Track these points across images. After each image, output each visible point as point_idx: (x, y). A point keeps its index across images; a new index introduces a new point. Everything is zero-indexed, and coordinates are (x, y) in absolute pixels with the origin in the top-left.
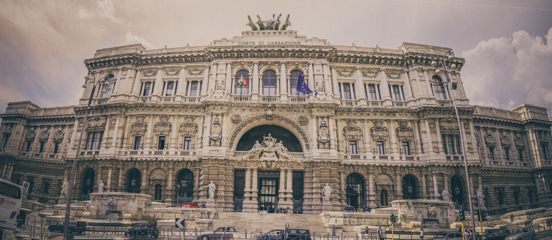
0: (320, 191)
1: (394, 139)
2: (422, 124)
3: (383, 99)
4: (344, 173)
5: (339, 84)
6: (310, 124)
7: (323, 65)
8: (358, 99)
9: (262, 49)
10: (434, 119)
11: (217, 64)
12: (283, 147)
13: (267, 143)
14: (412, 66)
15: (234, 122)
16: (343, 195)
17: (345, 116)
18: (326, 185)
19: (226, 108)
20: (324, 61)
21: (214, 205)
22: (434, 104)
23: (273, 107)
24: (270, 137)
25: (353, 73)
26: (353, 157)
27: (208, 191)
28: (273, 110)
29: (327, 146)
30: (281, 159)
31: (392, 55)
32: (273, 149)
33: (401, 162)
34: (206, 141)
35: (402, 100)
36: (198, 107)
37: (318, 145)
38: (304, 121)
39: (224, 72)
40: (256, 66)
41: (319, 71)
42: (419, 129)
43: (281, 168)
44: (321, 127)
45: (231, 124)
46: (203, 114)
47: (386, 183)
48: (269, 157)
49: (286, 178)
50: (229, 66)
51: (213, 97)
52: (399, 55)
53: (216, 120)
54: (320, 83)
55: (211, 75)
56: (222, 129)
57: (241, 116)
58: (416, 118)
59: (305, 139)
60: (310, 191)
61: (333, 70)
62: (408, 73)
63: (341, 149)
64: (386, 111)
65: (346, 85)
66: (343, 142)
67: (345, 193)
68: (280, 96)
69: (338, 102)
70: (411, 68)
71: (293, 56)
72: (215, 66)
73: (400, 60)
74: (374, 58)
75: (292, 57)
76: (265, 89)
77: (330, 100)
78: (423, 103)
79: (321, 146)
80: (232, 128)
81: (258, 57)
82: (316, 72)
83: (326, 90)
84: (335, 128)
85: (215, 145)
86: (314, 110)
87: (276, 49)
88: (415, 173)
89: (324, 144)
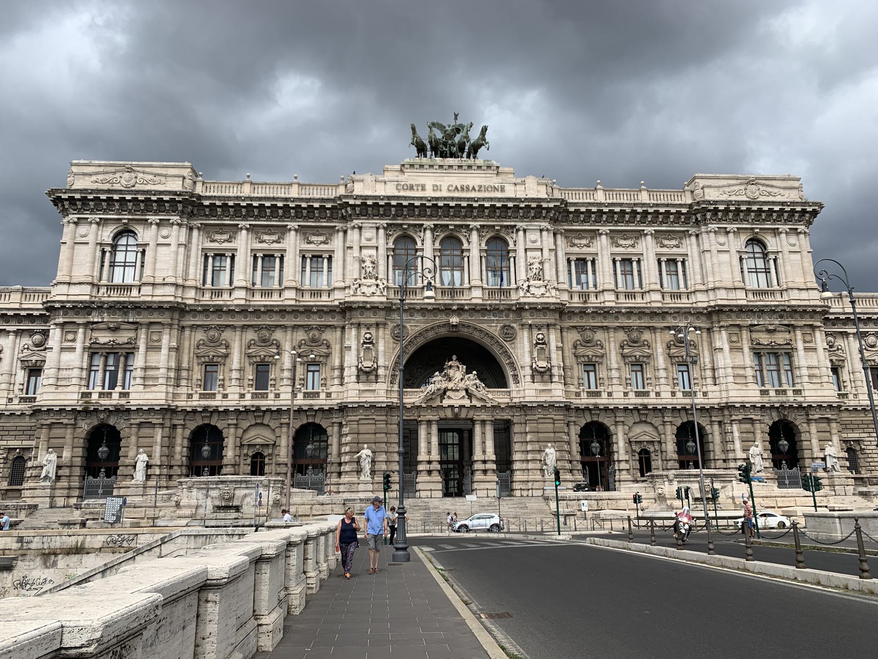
0: (538, 456)
1: (661, 361)
2: (717, 336)
3: (646, 288)
5: (569, 261)
6: (518, 338)
7: (541, 231)
8: (600, 288)
9: (441, 204)
10: (738, 325)
11: (360, 228)
12: (478, 381)
13: (451, 372)
14: (706, 225)
15: (396, 337)
16: (575, 463)
17: (576, 322)
18: (547, 447)
19: (382, 313)
20: (545, 224)
21: (370, 487)
22: (740, 299)
23: (461, 310)
24: (454, 363)
25: (595, 241)
26: (591, 394)
27: (358, 462)
28: (459, 315)
29: (546, 377)
30: (475, 402)
31: (668, 205)
32: (462, 385)
33: (675, 401)
34: (350, 373)
35: (683, 289)
36: (330, 311)
37: (533, 377)
38: (509, 334)
39: (373, 243)
40: (428, 233)
42: (711, 343)
43: (476, 418)
44: (537, 344)
45: (392, 341)
46: (341, 323)
47: (647, 438)
48: (456, 400)
49: (484, 433)
50: (381, 231)
51: (359, 293)
52: (681, 205)
53: (368, 336)
54: (536, 266)
55: (351, 248)
56: (377, 351)
57: (408, 325)
58: (705, 325)
59: (512, 364)
60: (523, 457)
61: (559, 237)
62: (697, 236)
63: (568, 380)
64: (648, 311)
65: (581, 262)
66: (572, 369)
67: (578, 457)
68: (470, 289)
69: (565, 297)
70: (703, 228)
72: (356, 231)
73: (683, 214)
74: (634, 213)
75: (489, 216)
76: (443, 272)
77: (552, 298)
78: (722, 298)
79: (538, 378)
80: (394, 349)
81: (430, 217)
82: (529, 245)
83: (547, 277)
84: (560, 345)
85: (368, 381)
86: (527, 315)
87: (464, 204)
88: (697, 419)
89: (542, 375)
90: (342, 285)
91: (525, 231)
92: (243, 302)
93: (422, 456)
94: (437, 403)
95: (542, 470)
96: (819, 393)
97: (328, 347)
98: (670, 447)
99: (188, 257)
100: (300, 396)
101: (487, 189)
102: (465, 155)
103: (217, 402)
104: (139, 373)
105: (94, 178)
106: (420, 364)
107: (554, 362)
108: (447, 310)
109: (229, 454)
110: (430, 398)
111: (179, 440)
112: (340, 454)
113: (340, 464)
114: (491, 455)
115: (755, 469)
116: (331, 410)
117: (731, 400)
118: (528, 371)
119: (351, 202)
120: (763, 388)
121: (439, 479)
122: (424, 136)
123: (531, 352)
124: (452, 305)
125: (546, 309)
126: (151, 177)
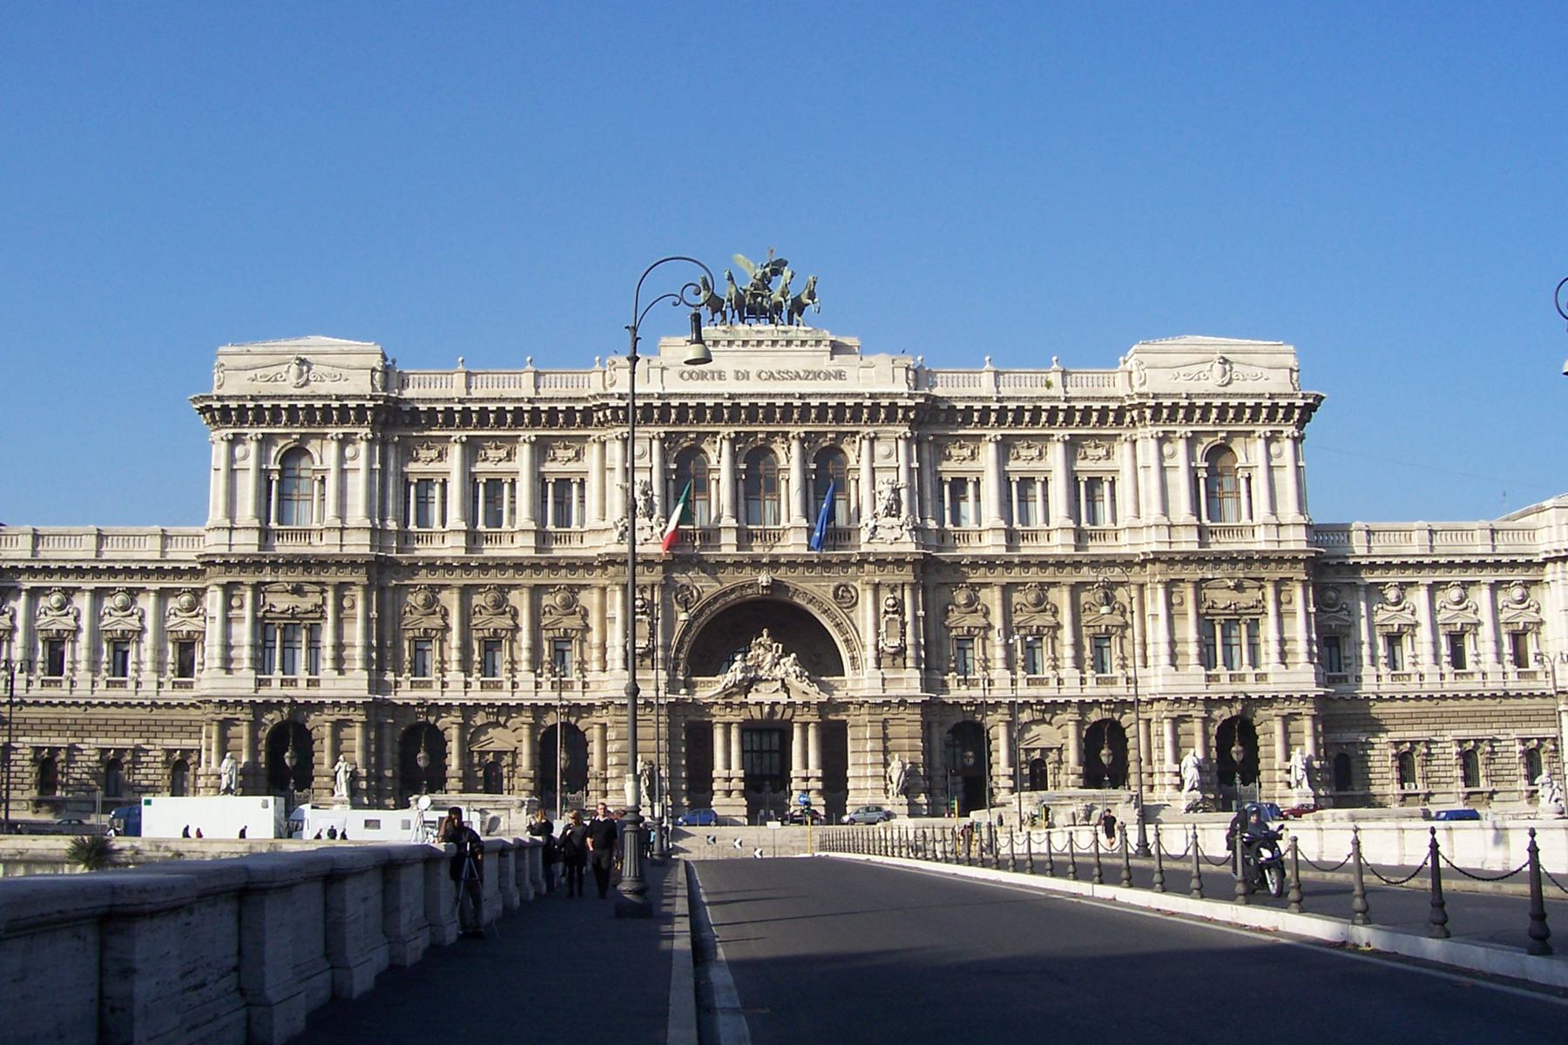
2: (1148, 593)
4: (941, 724)
24: (765, 639)
29: (899, 661)
31: (1088, 399)
34: (616, 655)
41: (889, 456)
44: (886, 612)
46: (603, 582)
48: (764, 694)
50: (656, 444)
54: (887, 494)
61: (925, 447)
71: (821, 418)
90: (602, 525)
91: (872, 441)
92: (462, 553)
93: (719, 770)
94: (737, 700)
95: (886, 791)
96: (1294, 678)
97: (585, 615)
98: (1072, 755)
99: (383, 486)
100: (547, 686)
101: (817, 375)
102: (785, 315)
103: (433, 694)
104: (327, 653)
105: (251, 374)
106: (719, 637)
107: (909, 639)
108: (756, 564)
109: (453, 762)
110: (727, 693)
111: (388, 746)
112: (604, 767)
113: (605, 780)
114: (814, 770)
115: (1187, 786)
116: (591, 707)
117: (1161, 690)
118: (870, 653)
119: (613, 403)
120: (1213, 672)
121: (744, 801)
122: (726, 292)
123: (877, 626)
124: (762, 556)
125: (899, 562)
126: (328, 370)
